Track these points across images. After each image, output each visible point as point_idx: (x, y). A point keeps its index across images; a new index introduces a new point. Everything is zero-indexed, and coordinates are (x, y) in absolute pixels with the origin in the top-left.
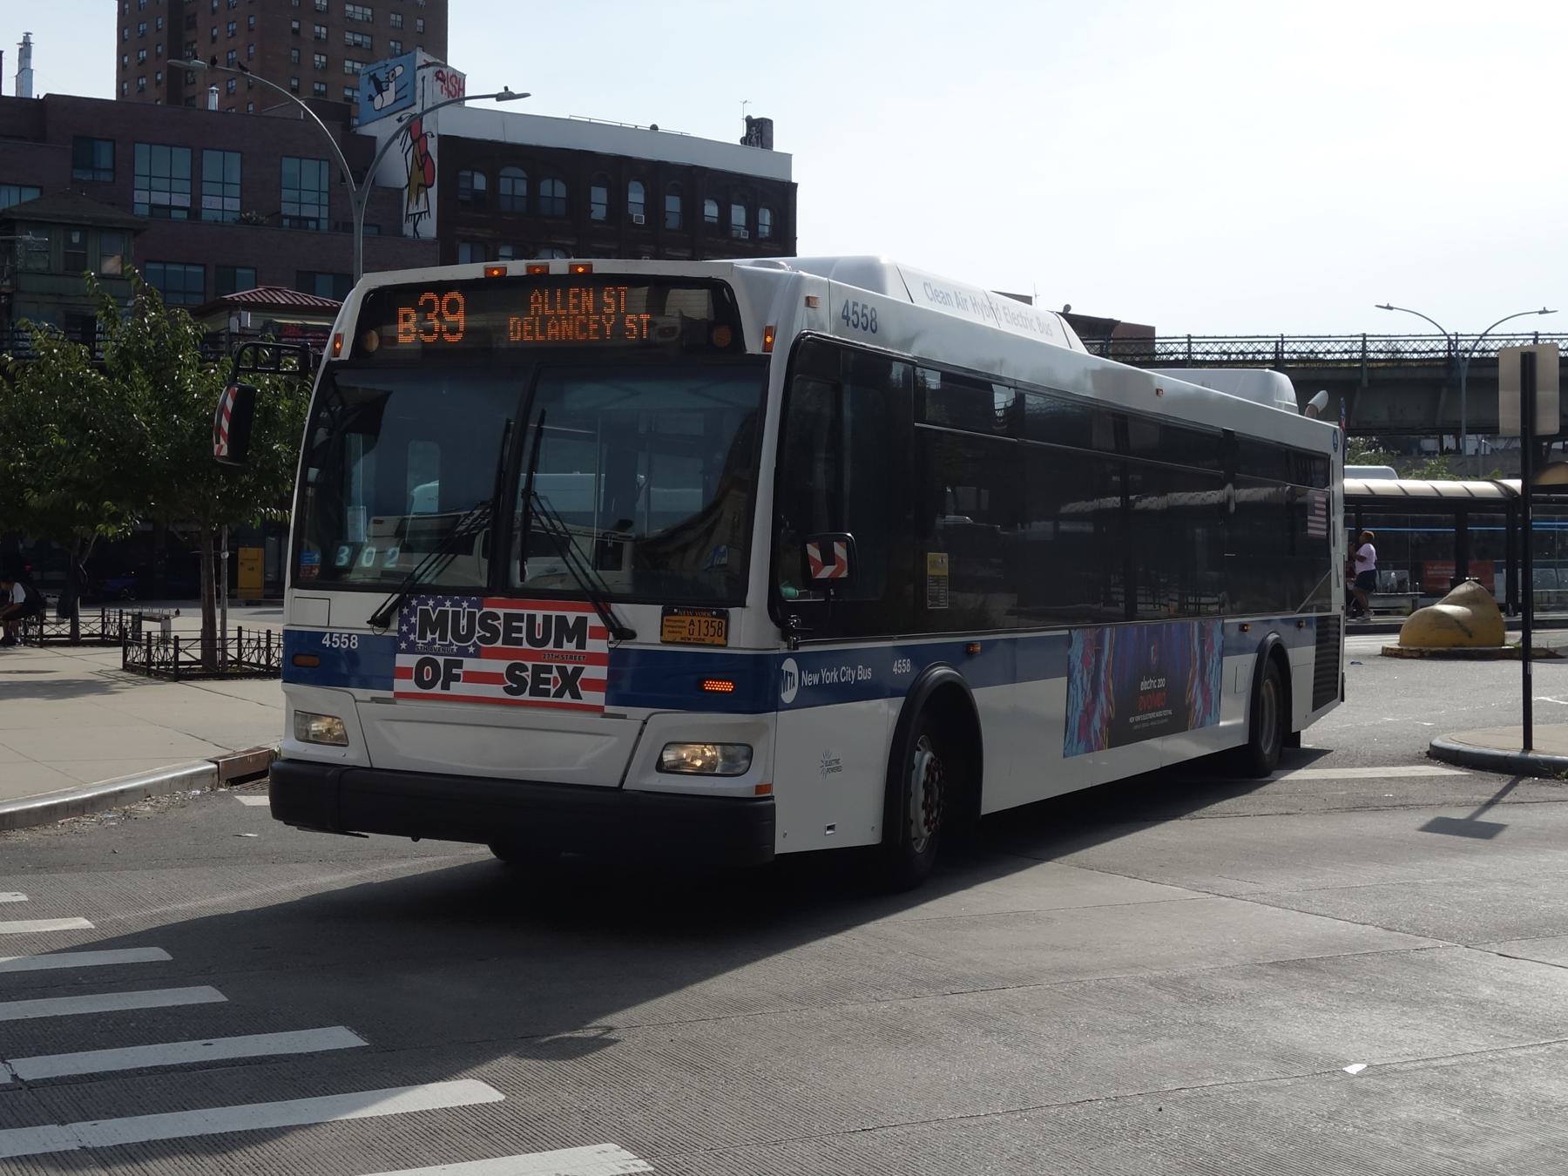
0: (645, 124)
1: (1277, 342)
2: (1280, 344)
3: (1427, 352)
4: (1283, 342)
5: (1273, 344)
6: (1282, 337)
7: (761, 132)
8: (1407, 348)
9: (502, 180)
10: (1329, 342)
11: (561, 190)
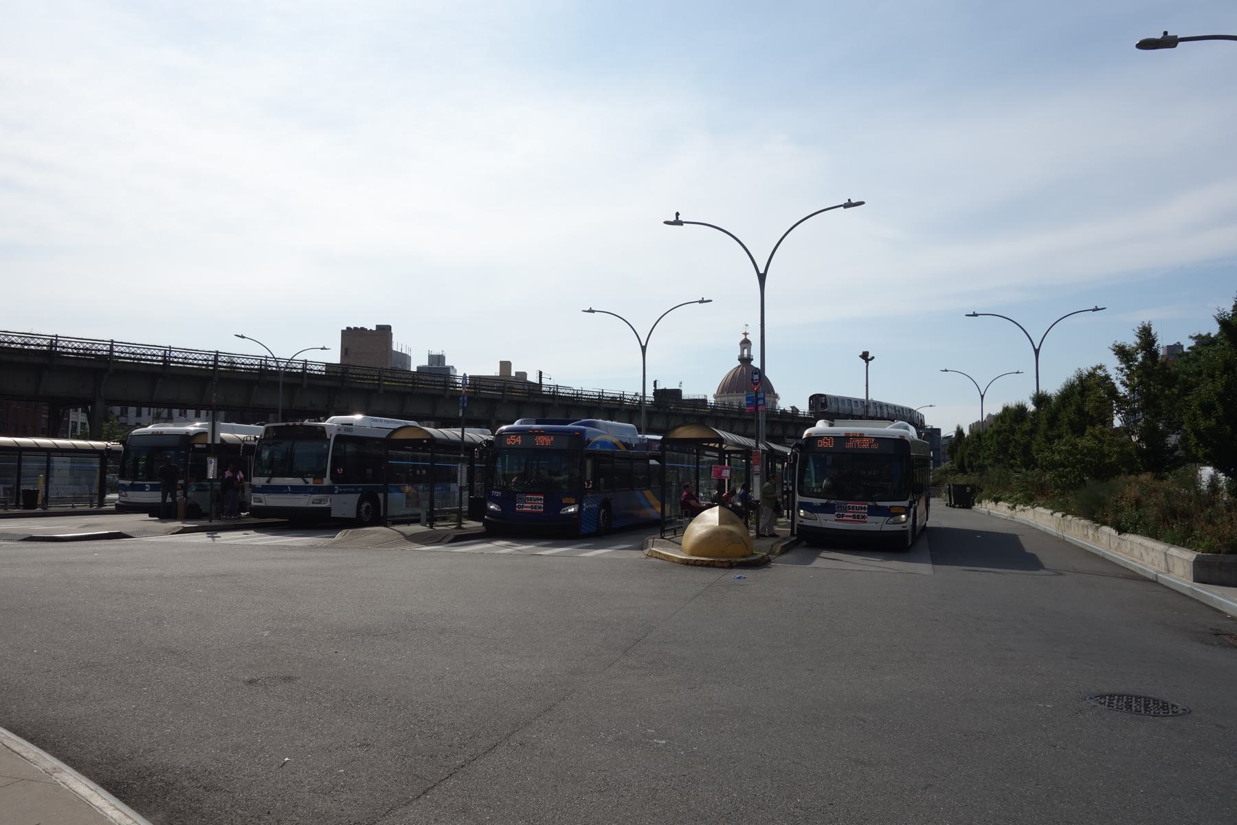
1: (165, 351)
2: (168, 352)
3: (249, 365)
4: (170, 351)
5: (163, 351)
6: (170, 347)
8: (239, 361)
10: (196, 353)
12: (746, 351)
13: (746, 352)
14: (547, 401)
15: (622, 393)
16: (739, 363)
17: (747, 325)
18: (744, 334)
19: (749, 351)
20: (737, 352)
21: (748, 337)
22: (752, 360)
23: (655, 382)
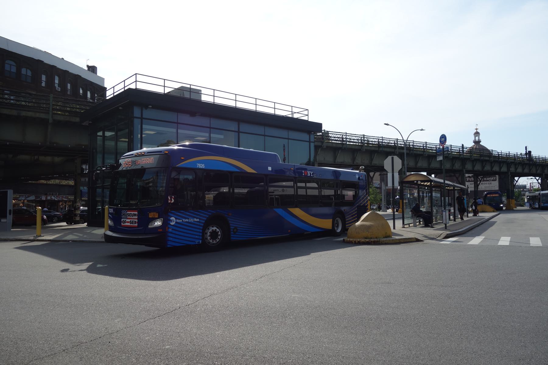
0: (61, 58)
5: (342, 136)
6: (346, 133)
7: (94, 70)
8: (370, 140)
9: (6, 64)
11: (29, 73)
12: (477, 138)
13: (477, 138)
14: (487, 158)
15: (516, 153)
16: (473, 144)
17: (477, 125)
18: (475, 129)
19: (479, 138)
20: (473, 138)
21: (478, 131)
22: (481, 142)
23: (526, 147)
